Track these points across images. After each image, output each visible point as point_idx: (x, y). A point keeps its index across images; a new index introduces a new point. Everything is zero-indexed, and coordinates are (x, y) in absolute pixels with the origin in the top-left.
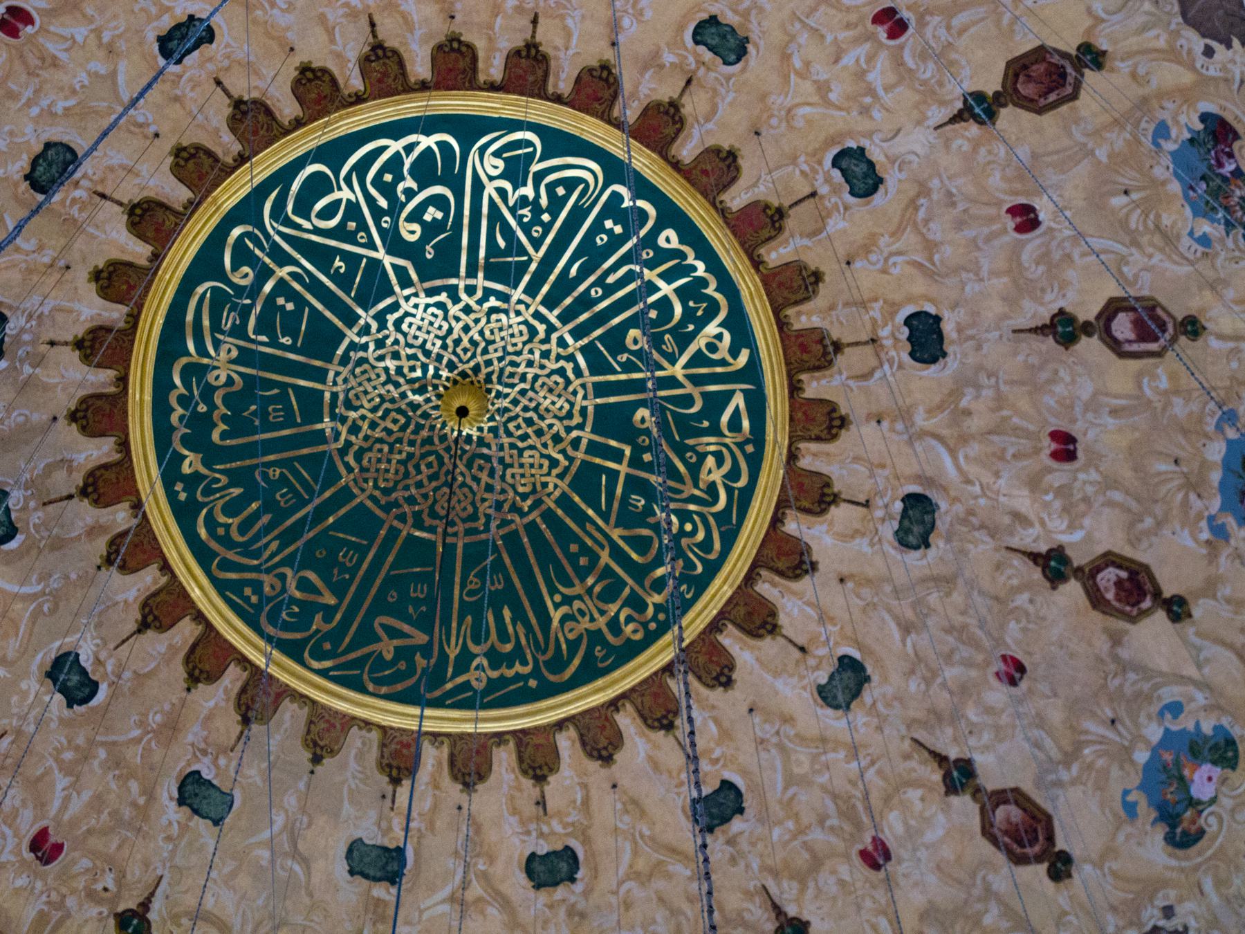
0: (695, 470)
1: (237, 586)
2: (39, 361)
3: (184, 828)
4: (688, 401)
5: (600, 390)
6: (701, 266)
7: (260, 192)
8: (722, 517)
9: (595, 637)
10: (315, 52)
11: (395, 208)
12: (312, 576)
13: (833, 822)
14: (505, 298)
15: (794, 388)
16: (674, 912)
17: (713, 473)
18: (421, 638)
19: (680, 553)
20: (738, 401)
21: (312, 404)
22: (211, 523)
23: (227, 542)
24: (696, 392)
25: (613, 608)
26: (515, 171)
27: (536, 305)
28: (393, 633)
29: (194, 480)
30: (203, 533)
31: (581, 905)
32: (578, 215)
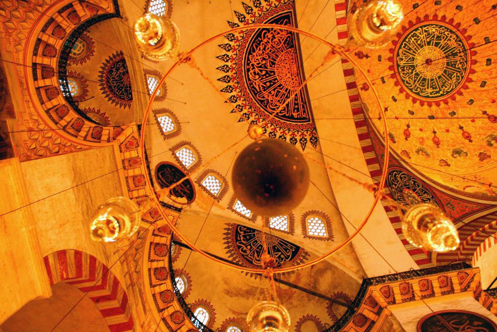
0: (434, 32)
1: (456, 85)
2: (433, 112)
3: (487, 86)
4: (425, 35)
5: (425, 45)
6: (410, 36)
7: (409, 89)
8: (439, 28)
9: (456, 41)
10: (393, 84)
11: (408, 73)
12: (453, 76)
13: (478, 5)
14: (416, 59)
15: (423, 22)
16: (492, 23)
17: (434, 30)
18: (458, 62)
19: (444, 33)
20: (425, 28)
21: (432, 80)
22: (448, 89)
23: (450, 87)
24: (424, 34)
25: (452, 40)
26: (402, 59)
27: (416, 55)
28: (458, 65)
29: (444, 92)
30: (449, 90)
31: (491, 35)
32: (405, 51)
